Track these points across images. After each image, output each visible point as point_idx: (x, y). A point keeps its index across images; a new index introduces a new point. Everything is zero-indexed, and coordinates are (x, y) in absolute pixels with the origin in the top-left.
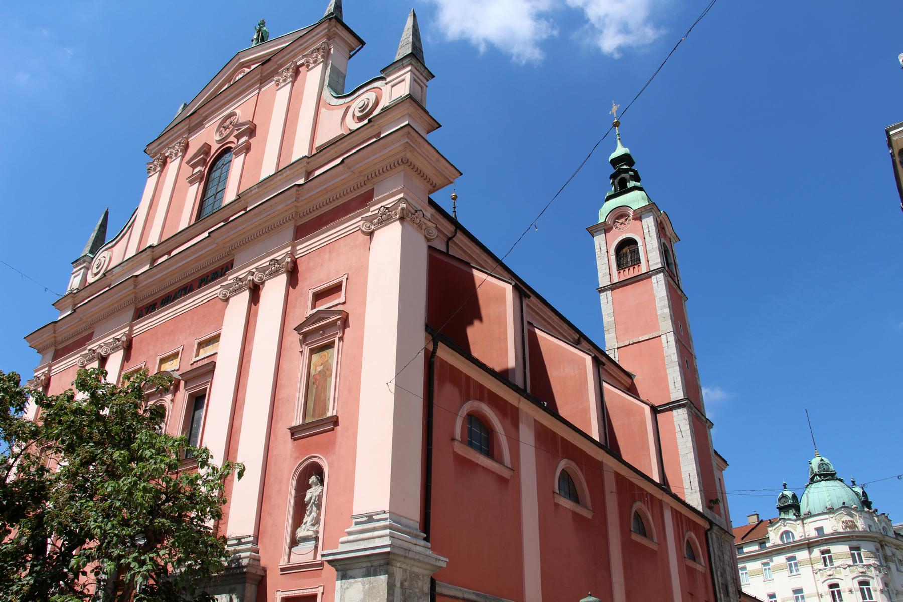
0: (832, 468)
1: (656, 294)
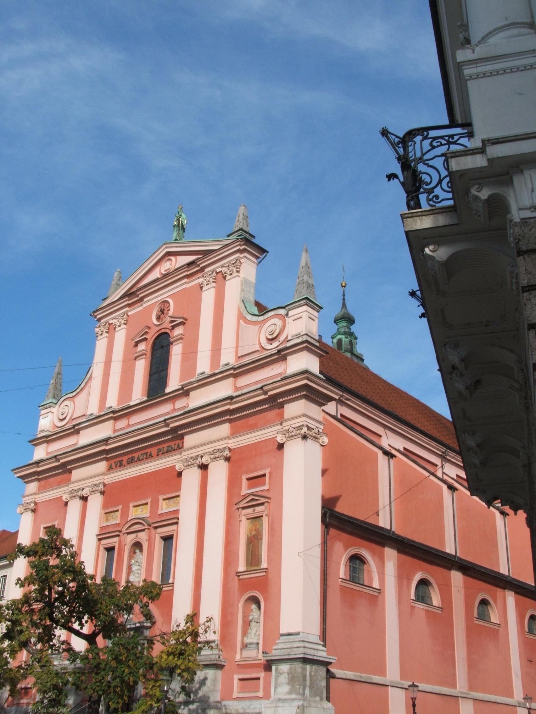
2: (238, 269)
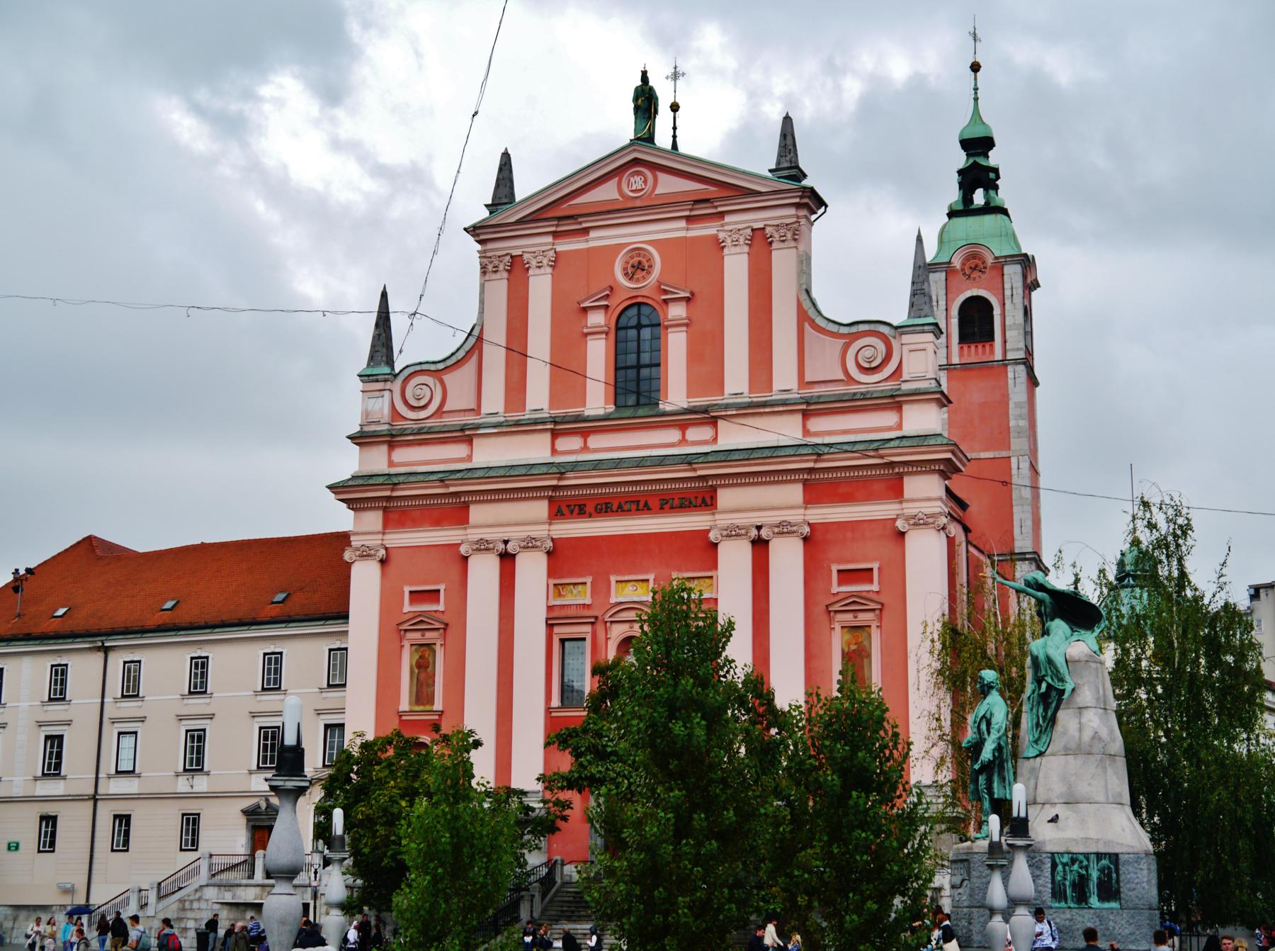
1: (1011, 396)
2: (796, 237)
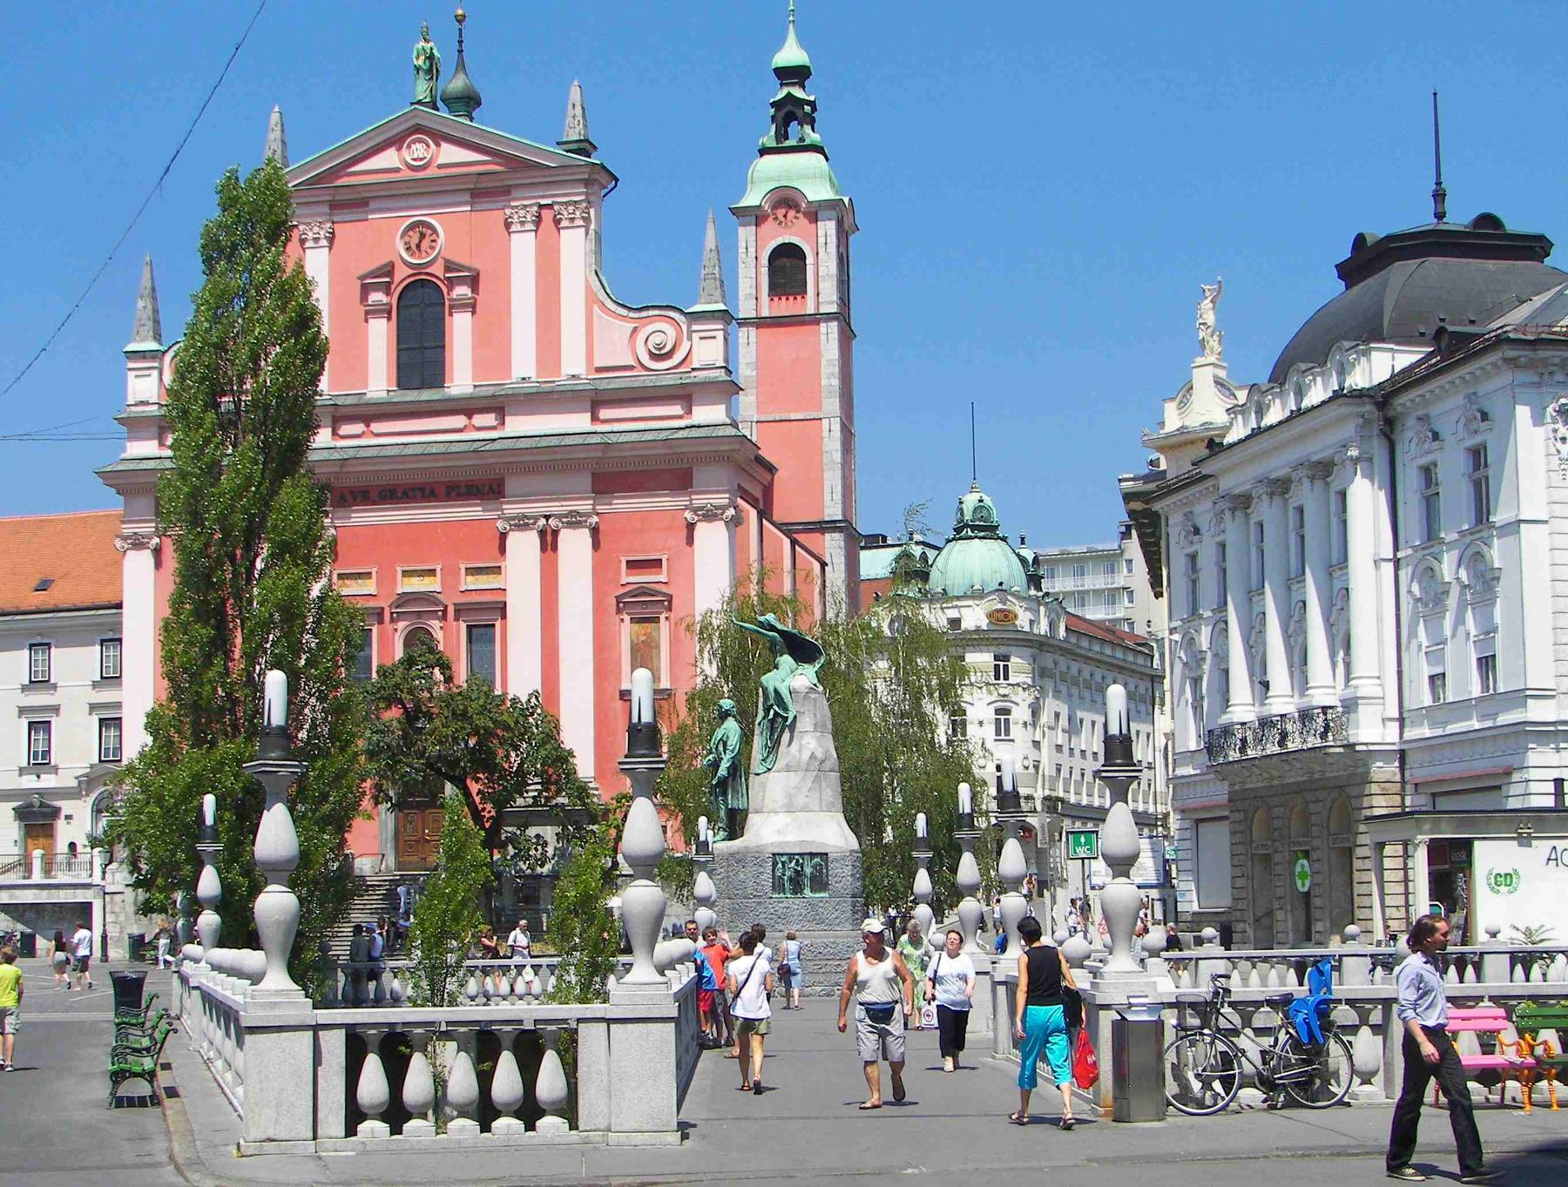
0: (995, 518)
